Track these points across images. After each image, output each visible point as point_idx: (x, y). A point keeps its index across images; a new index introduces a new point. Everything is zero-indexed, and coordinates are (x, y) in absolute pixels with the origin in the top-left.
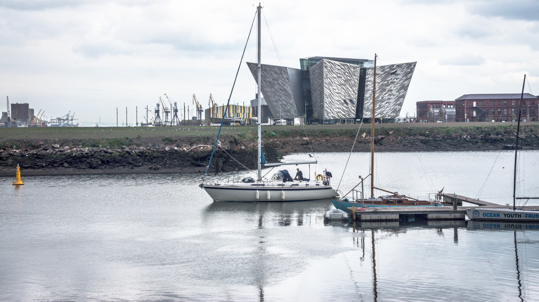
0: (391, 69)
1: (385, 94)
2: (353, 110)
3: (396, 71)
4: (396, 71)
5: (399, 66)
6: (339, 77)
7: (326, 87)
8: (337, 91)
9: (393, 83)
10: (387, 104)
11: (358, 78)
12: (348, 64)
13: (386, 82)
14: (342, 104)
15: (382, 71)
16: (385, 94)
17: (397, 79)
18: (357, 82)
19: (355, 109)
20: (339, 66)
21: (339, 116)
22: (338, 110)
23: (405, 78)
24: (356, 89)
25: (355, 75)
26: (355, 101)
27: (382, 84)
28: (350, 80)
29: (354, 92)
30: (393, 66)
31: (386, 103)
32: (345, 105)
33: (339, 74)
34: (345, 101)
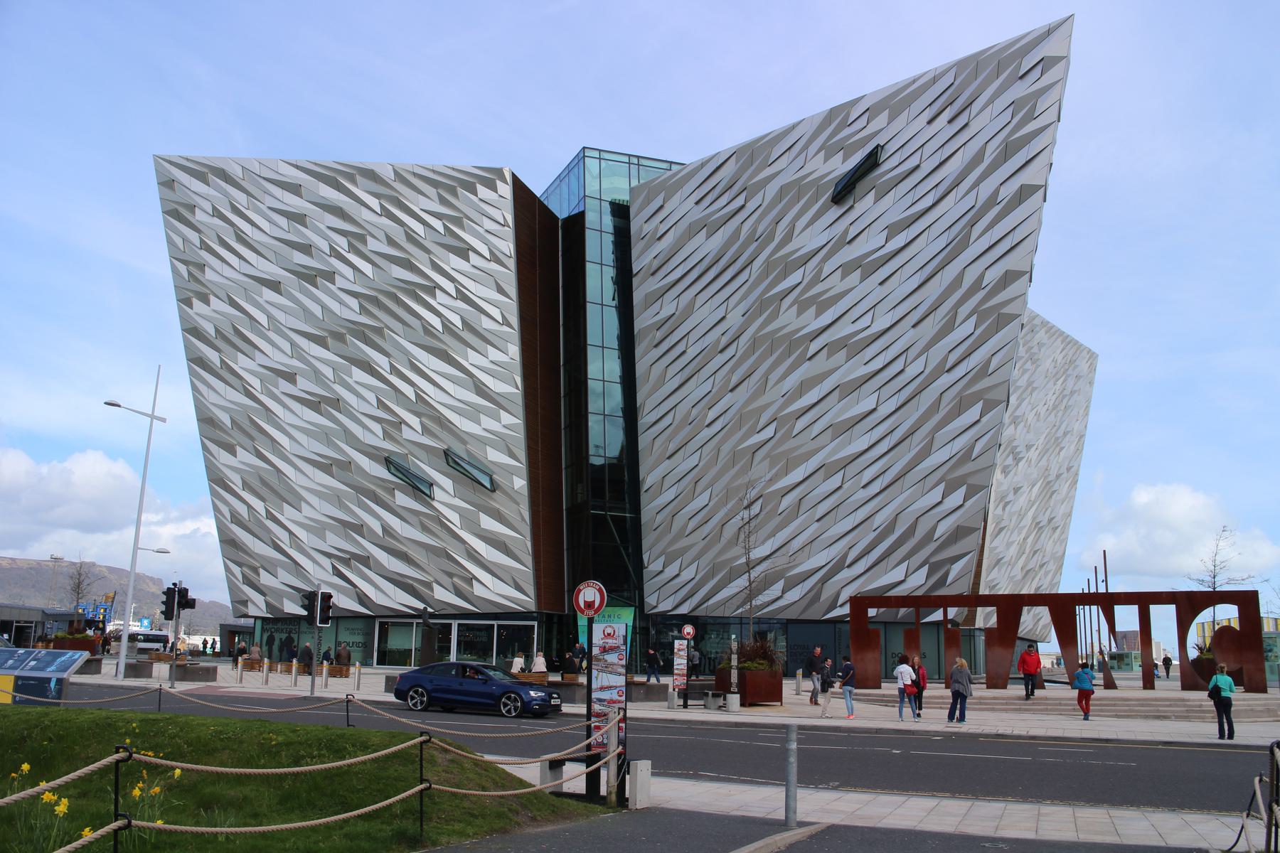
0: (829, 151)
1: (803, 388)
3: (872, 162)
4: (872, 162)
5: (895, 102)
8: (305, 385)
9: (866, 266)
10: (835, 481)
15: (750, 191)
16: (803, 388)
18: (499, 306)
19: (522, 539)
20: (295, 189)
21: (362, 599)
22: (334, 541)
24: (500, 362)
25: (464, 252)
27: (762, 305)
29: (481, 390)
30: (838, 116)
31: (827, 470)
32: (402, 500)
33: (306, 249)
34: (388, 462)
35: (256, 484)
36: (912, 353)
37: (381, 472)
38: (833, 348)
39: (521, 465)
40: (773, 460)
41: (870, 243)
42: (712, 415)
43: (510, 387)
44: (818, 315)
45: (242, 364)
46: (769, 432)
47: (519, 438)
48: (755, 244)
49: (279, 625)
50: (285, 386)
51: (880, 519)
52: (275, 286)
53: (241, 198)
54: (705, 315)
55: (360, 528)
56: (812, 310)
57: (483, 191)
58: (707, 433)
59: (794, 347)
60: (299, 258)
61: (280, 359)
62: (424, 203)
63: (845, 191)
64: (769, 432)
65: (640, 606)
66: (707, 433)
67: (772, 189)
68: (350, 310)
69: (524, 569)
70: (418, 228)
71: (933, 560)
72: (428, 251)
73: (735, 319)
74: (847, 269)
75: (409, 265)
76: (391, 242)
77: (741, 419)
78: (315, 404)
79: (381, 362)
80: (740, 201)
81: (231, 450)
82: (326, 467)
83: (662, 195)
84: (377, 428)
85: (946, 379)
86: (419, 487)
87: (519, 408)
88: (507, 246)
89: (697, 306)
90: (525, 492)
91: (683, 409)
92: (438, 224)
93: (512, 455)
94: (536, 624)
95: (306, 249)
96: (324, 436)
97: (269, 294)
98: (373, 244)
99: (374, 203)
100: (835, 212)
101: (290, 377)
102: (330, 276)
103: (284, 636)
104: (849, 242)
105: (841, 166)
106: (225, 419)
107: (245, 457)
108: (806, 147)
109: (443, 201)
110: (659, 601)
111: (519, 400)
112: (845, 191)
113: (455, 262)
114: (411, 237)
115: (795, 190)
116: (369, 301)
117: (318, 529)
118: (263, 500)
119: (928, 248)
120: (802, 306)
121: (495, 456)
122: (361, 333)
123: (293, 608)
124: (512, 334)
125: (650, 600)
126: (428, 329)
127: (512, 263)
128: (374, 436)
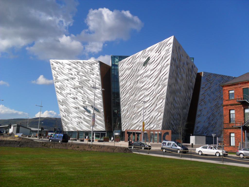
0: (143, 57)
2: (100, 120)
3: (149, 59)
4: (149, 59)
6: (73, 79)
7: (58, 92)
8: (72, 96)
9: (148, 76)
11: (99, 77)
12: (81, 61)
13: (139, 78)
14: (83, 112)
15: (133, 63)
17: (152, 70)
18: (98, 83)
23: (159, 67)
24: (99, 92)
25: (93, 74)
26: (101, 108)
28: (86, 80)
31: (144, 109)
32: (86, 113)
33: (72, 74)
34: (84, 107)
35: (66, 111)
36: (154, 90)
37: (83, 109)
38: (144, 89)
39: (102, 108)
40: (137, 107)
41: (148, 73)
42: (129, 100)
43: (100, 96)
44: (142, 84)
45: (63, 92)
46: (136, 103)
47: (102, 104)
48: (134, 72)
49: (70, 133)
50: (69, 95)
51: (151, 116)
52: (68, 80)
53: (62, 66)
54: (128, 83)
55: (81, 118)
56: (141, 83)
57: (95, 64)
58: (129, 102)
59: (140, 89)
60: (70, 76)
61: (68, 91)
62: (87, 67)
63: (145, 63)
64: (136, 103)
65: (121, 130)
66: (129, 102)
67: (136, 63)
68: (77, 84)
69: (104, 124)
70: (86, 71)
71: (157, 123)
72: (88, 74)
73: (132, 85)
74: (145, 77)
75: (85, 76)
76: (83, 73)
77: (133, 100)
78: (74, 99)
79: (82, 92)
80: (132, 65)
81: (63, 105)
82: (76, 108)
83: (122, 64)
84: (82, 102)
85: (158, 95)
86: (89, 112)
87: (102, 99)
88: (99, 73)
89: (127, 81)
90: (103, 112)
91: (126, 99)
92: (89, 70)
93: (101, 106)
94: (106, 133)
95: (72, 74)
96: (75, 103)
97: (66, 81)
98: (81, 73)
99: (80, 67)
100: (144, 67)
101: (70, 94)
102: (75, 78)
103: (71, 134)
104: (146, 72)
105: (145, 60)
106: (61, 101)
107: (64, 107)
108: (140, 56)
109: (90, 66)
110: (124, 129)
111: (102, 97)
112: (145, 63)
113: (92, 76)
114: (85, 72)
115: (139, 63)
116: (80, 83)
117: (75, 118)
118: (67, 113)
119: (156, 73)
120: (140, 83)
121: (99, 106)
122: (80, 87)
123: (72, 130)
124: (100, 87)
125: (123, 129)
126: (89, 87)
127: (100, 76)
128: (82, 104)
